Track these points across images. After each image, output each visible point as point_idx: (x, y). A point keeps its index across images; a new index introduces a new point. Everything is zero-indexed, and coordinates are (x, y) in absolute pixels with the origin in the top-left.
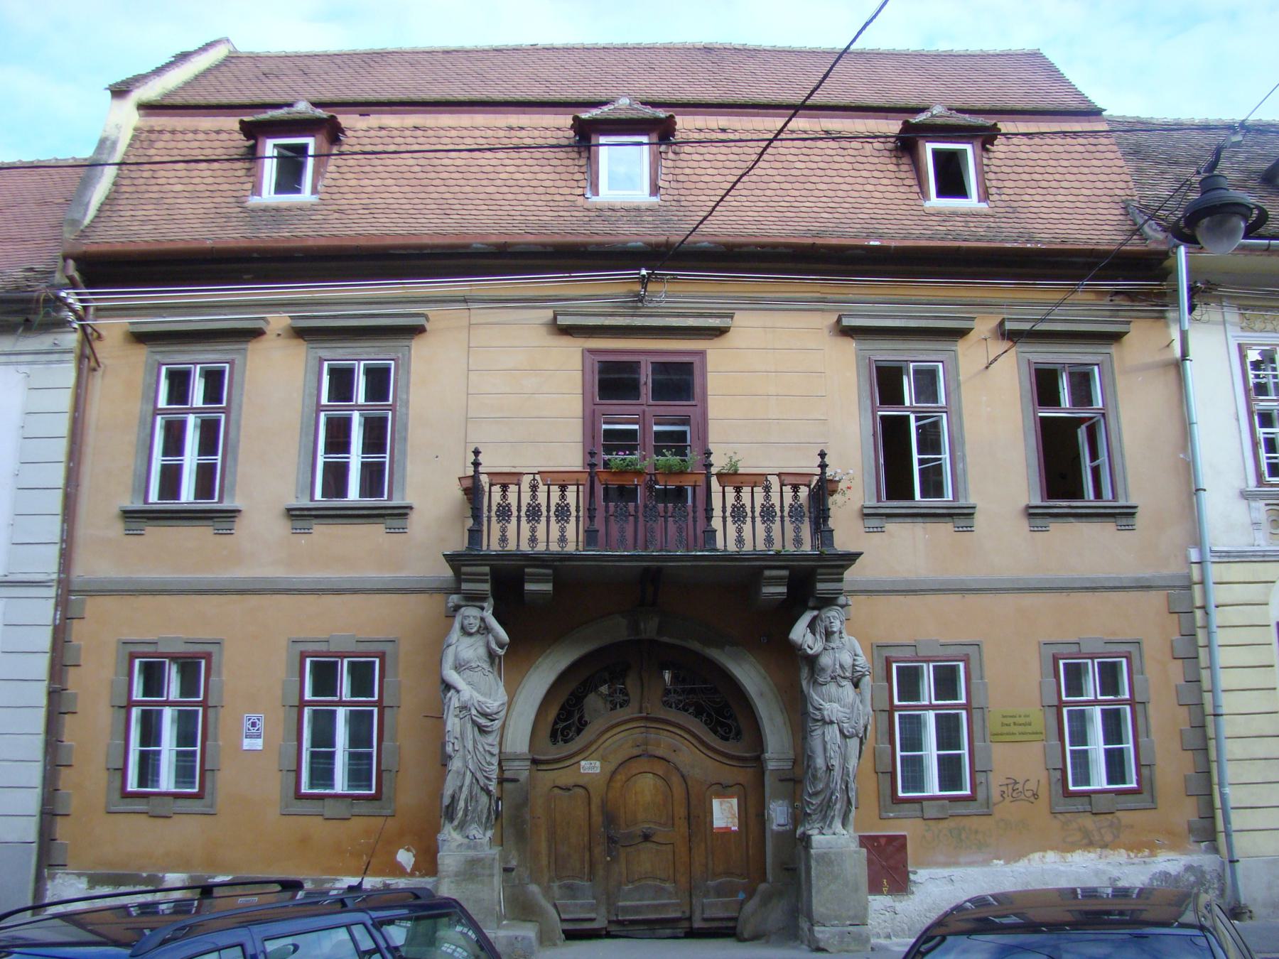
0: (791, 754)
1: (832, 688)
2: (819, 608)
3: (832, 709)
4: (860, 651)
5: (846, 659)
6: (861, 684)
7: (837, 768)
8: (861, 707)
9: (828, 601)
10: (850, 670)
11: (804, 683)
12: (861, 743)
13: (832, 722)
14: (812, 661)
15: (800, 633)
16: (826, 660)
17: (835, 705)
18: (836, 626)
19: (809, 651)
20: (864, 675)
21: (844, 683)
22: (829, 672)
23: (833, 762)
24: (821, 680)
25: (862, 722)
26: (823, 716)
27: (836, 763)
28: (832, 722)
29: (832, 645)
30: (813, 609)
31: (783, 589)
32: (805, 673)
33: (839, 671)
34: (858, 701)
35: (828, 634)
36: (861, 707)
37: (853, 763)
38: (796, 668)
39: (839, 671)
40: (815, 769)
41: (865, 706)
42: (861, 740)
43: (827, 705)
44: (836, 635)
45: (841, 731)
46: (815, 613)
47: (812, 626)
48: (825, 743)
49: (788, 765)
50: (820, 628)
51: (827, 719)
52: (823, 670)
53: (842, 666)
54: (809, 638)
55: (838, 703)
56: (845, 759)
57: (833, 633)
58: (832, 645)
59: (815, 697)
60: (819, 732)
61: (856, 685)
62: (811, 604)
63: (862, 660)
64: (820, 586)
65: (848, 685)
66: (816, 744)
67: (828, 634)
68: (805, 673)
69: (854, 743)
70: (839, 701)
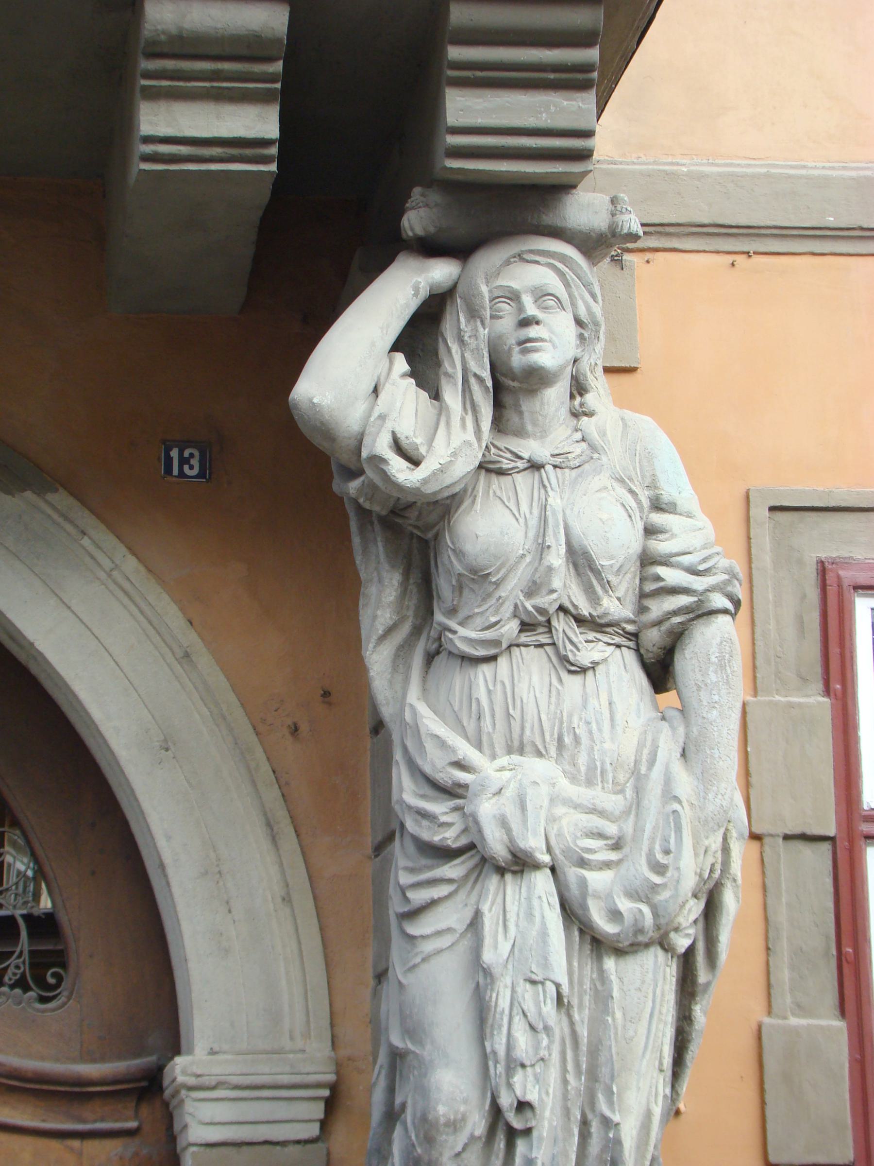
0: (315, 1063)
1: (528, 676)
2: (460, 250)
3: (520, 795)
4: (677, 485)
5: (614, 535)
6: (686, 664)
7: (547, 1121)
8: (685, 783)
9: (513, 205)
10: (626, 585)
11: (378, 660)
12: (687, 988)
13: (520, 864)
14: (417, 531)
15: (349, 372)
16: (491, 527)
17: (540, 770)
18: (554, 345)
19: (400, 471)
20: (702, 612)
21: (590, 649)
22: (512, 590)
23: (525, 1086)
24: (464, 636)
25: (688, 869)
26: (472, 824)
27: (543, 1088)
28: (520, 864)
29: (531, 448)
30: (430, 248)
31: (262, 123)
32: (382, 599)
33: (566, 587)
34: (668, 746)
35: (510, 389)
36: (685, 783)
37: (639, 1097)
38: (324, 553)
39: (566, 587)
40: (428, 1130)
41: (706, 778)
42: (687, 960)
43: (491, 770)
44: (555, 396)
45: (572, 913)
46: (441, 272)
47: (420, 340)
48: (480, 979)
49: (301, 1118)
50: (464, 353)
51: (496, 844)
52: (479, 578)
53: (580, 560)
54: (404, 405)
55: (544, 752)
56: (595, 1071)
57: (536, 379)
58: (531, 448)
59: (432, 723)
60: (451, 917)
61: (660, 672)
62: (415, 221)
63: (692, 535)
64: (463, 107)
65: (620, 673)
66: (435, 983)
67: (510, 389)
68: (382, 599)
69: (644, 985)
70: (563, 746)
